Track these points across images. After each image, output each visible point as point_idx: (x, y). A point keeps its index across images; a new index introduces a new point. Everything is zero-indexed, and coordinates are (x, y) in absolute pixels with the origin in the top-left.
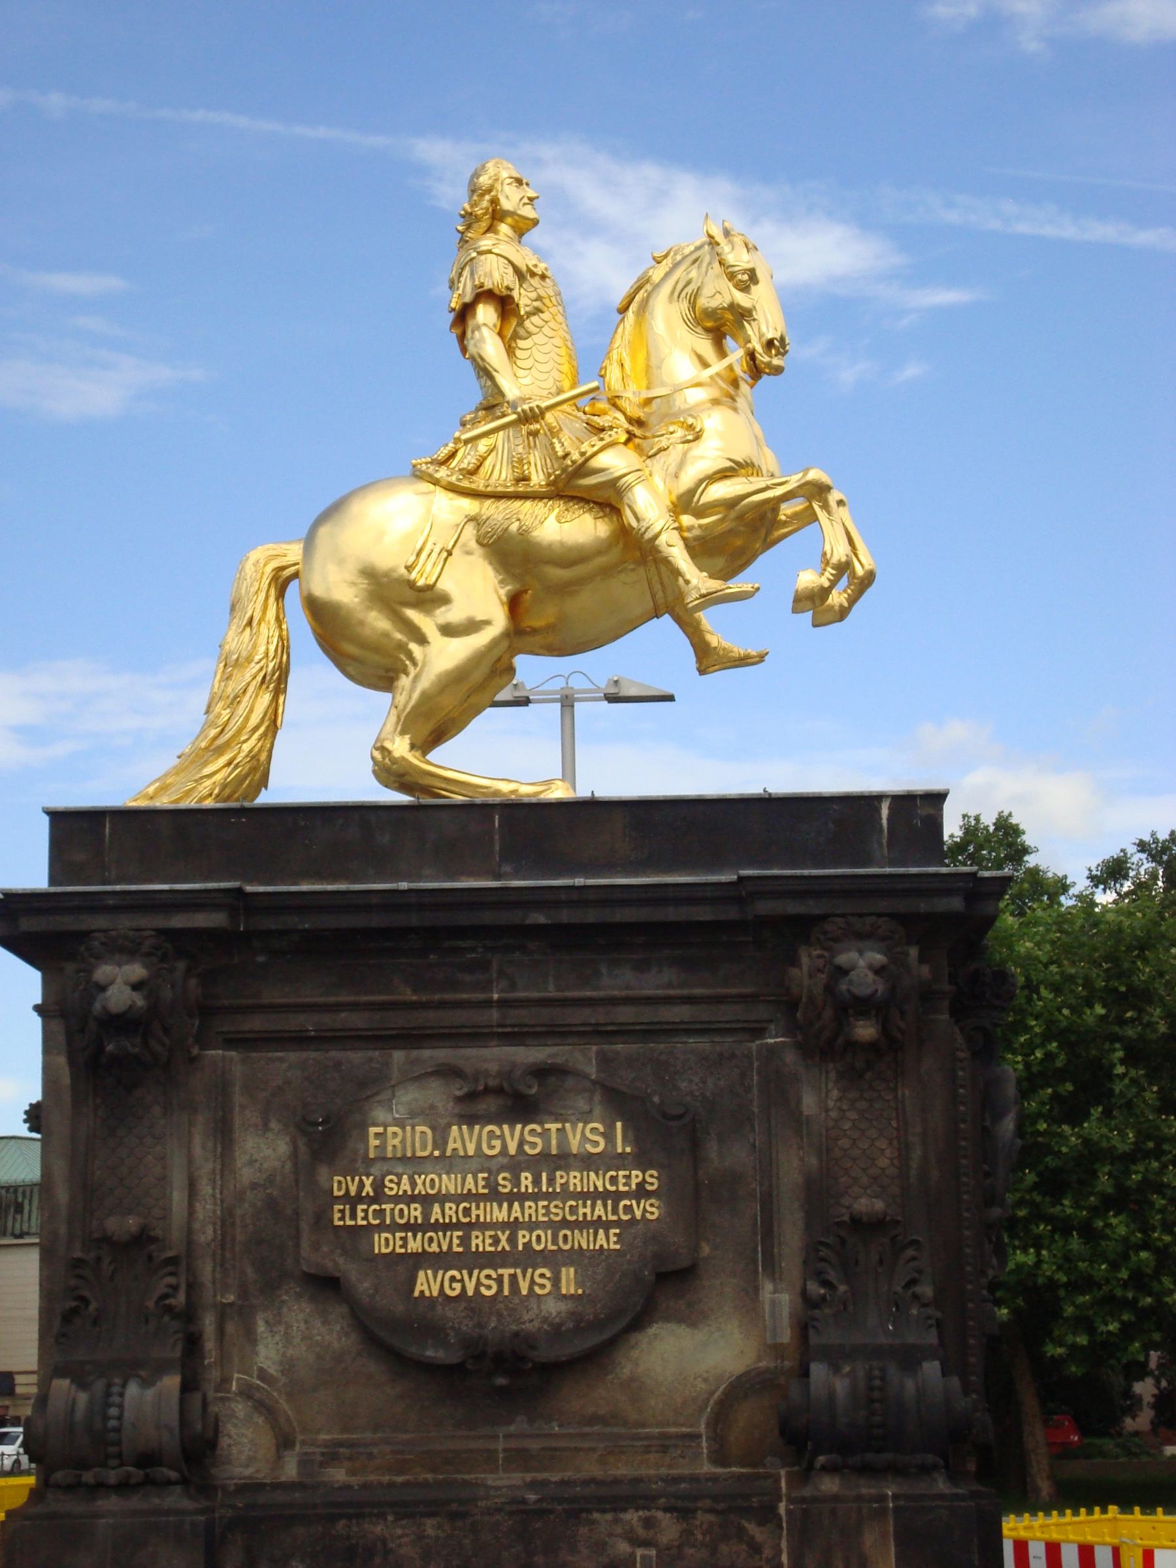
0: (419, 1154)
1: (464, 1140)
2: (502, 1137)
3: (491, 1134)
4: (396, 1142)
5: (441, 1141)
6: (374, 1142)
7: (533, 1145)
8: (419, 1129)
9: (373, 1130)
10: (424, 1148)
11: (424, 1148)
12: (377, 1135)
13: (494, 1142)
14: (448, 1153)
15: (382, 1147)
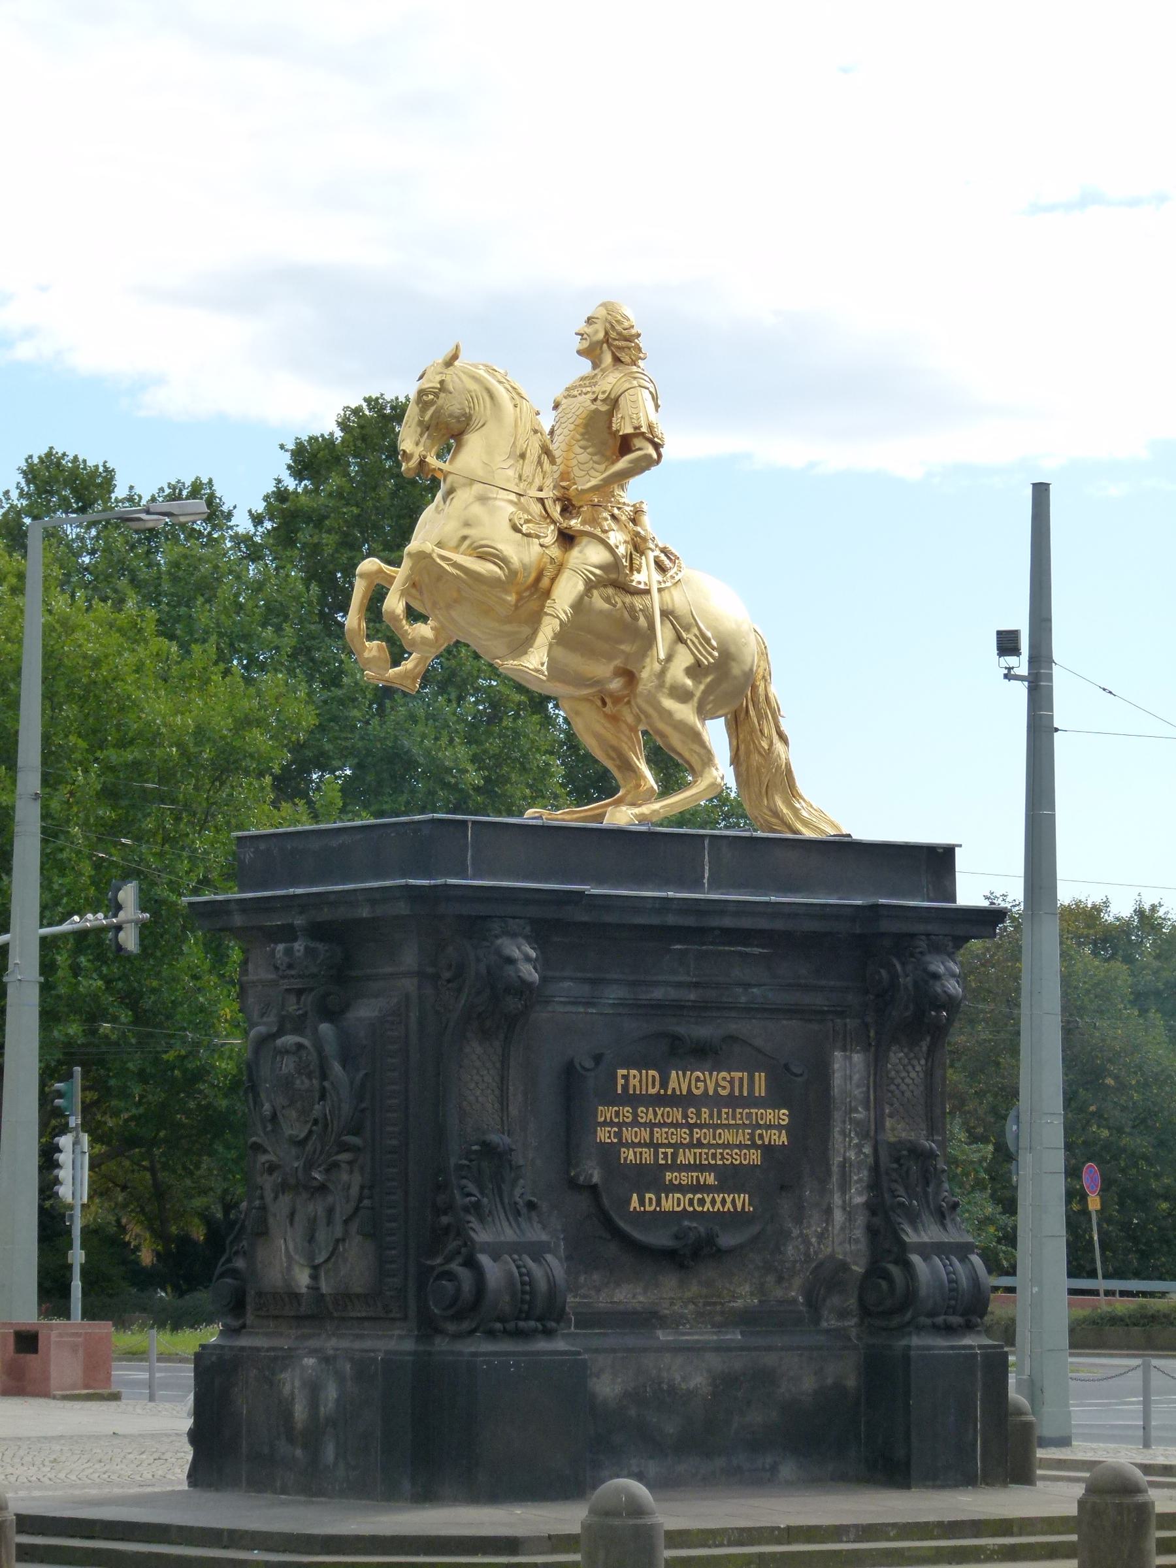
0: (652, 1091)
1: (678, 1082)
2: (705, 1081)
3: (698, 1079)
4: (636, 1082)
5: (664, 1083)
6: (621, 1082)
7: (724, 1088)
8: (651, 1072)
9: (621, 1072)
10: (653, 1087)
11: (653, 1087)
12: (623, 1076)
13: (700, 1084)
14: (669, 1092)
15: (625, 1087)
